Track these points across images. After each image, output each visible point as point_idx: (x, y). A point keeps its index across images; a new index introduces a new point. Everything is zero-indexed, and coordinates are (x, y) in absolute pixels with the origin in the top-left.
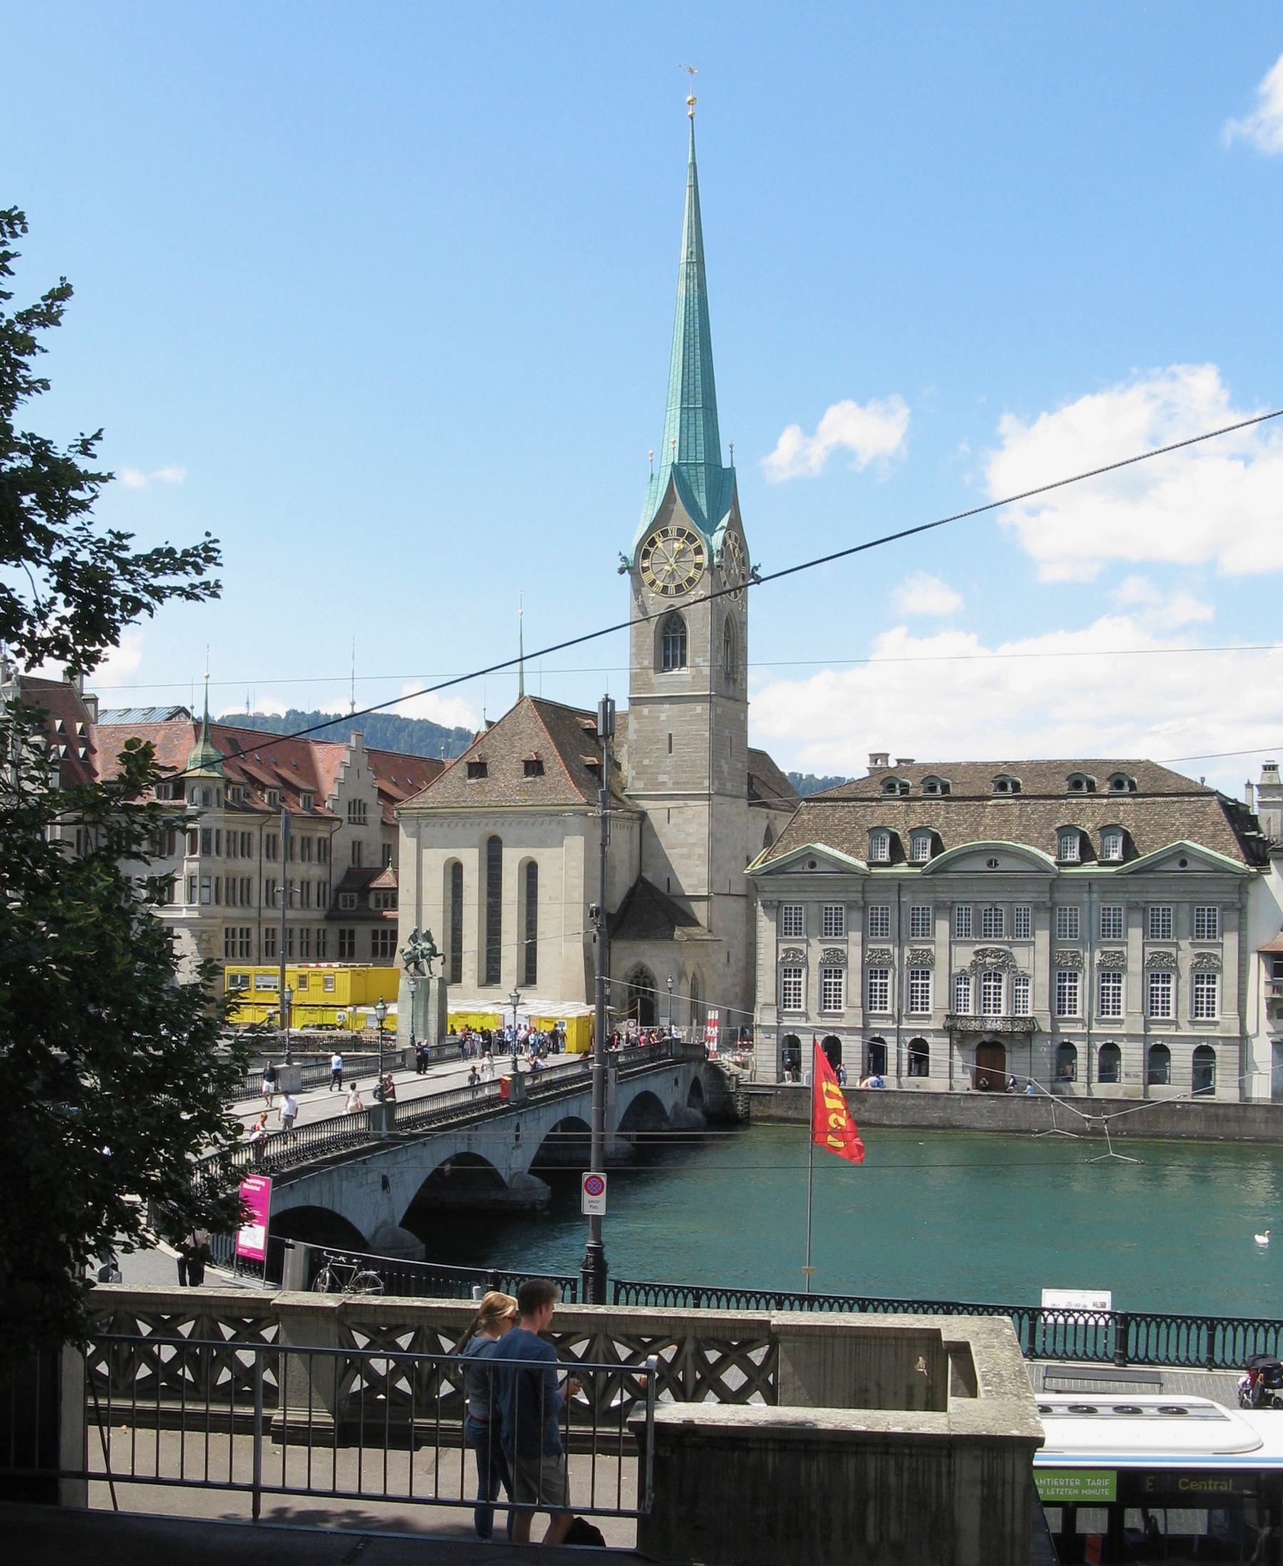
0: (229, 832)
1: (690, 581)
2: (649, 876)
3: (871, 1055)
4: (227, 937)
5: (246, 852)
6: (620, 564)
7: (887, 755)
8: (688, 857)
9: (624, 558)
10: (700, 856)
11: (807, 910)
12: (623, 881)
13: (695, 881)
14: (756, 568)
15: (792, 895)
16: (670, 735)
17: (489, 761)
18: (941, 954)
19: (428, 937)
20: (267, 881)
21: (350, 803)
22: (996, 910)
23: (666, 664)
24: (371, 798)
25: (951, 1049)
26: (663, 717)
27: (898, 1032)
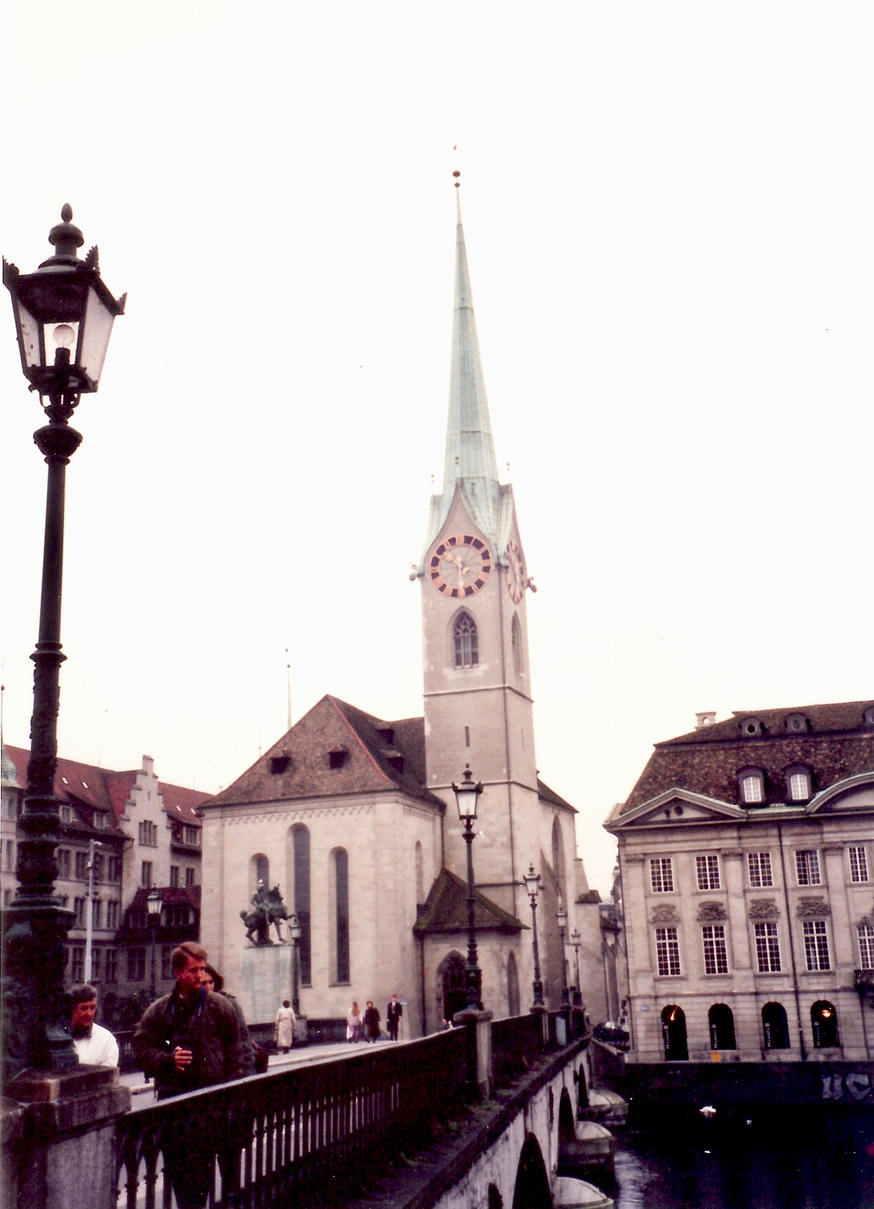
3: (767, 1025)
7: (714, 714)
8: (490, 845)
9: (414, 566)
10: (502, 844)
11: (676, 861)
12: (431, 873)
13: (500, 870)
15: (659, 846)
17: (293, 756)
18: (837, 902)
19: (275, 895)
21: (140, 824)
23: (458, 661)
24: (161, 821)
25: (863, 1012)
27: (797, 993)
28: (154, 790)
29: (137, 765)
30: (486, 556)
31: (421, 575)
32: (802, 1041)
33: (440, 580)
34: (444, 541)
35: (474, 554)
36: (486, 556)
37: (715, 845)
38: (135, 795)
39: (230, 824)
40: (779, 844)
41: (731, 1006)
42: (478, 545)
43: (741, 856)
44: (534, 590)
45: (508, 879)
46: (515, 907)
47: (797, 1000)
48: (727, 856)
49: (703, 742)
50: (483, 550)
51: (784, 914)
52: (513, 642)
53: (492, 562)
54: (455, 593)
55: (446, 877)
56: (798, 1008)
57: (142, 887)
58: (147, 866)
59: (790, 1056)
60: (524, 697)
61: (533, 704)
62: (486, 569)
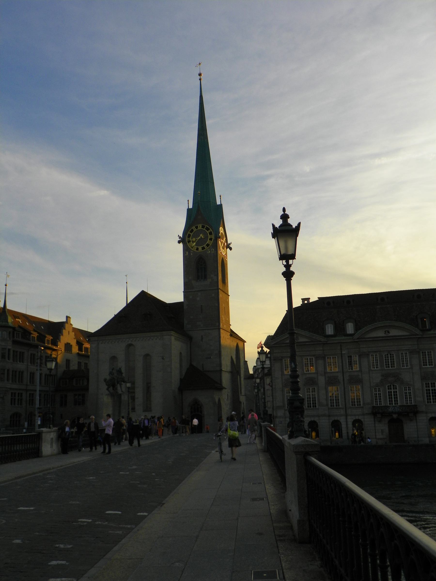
0: (14, 351)
1: (208, 245)
2: (194, 364)
3: (333, 429)
4: (12, 396)
5: (22, 360)
6: (179, 239)
7: (309, 299)
9: (180, 237)
14: (230, 244)
16: (202, 306)
20: (31, 373)
21: (65, 344)
22: (390, 355)
24: (73, 343)
26: (198, 299)
27: (346, 415)
28: (71, 330)
29: (64, 320)
39: (102, 343)
40: (340, 353)
41: (317, 421)
44: (231, 249)
47: (346, 419)
50: (209, 231)
56: (347, 422)
57: (65, 369)
60: (226, 293)
61: (229, 297)
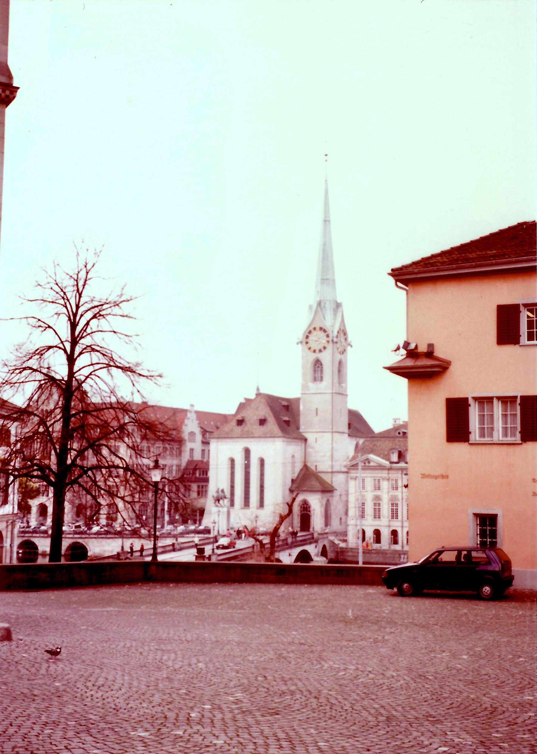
23: (315, 379)
27: (402, 527)
30: (328, 336)
31: (301, 342)
32: (402, 543)
33: (309, 345)
34: (311, 328)
35: (322, 334)
36: (328, 336)
37: (380, 475)
38: (186, 421)
42: (325, 331)
43: (388, 480)
44: (351, 346)
45: (330, 470)
46: (332, 481)
48: (384, 479)
49: (383, 437)
50: (326, 334)
51: (401, 500)
52: (339, 371)
53: (330, 339)
54: (314, 351)
55: (306, 467)
58: (192, 450)
59: (398, 547)
62: (328, 342)
